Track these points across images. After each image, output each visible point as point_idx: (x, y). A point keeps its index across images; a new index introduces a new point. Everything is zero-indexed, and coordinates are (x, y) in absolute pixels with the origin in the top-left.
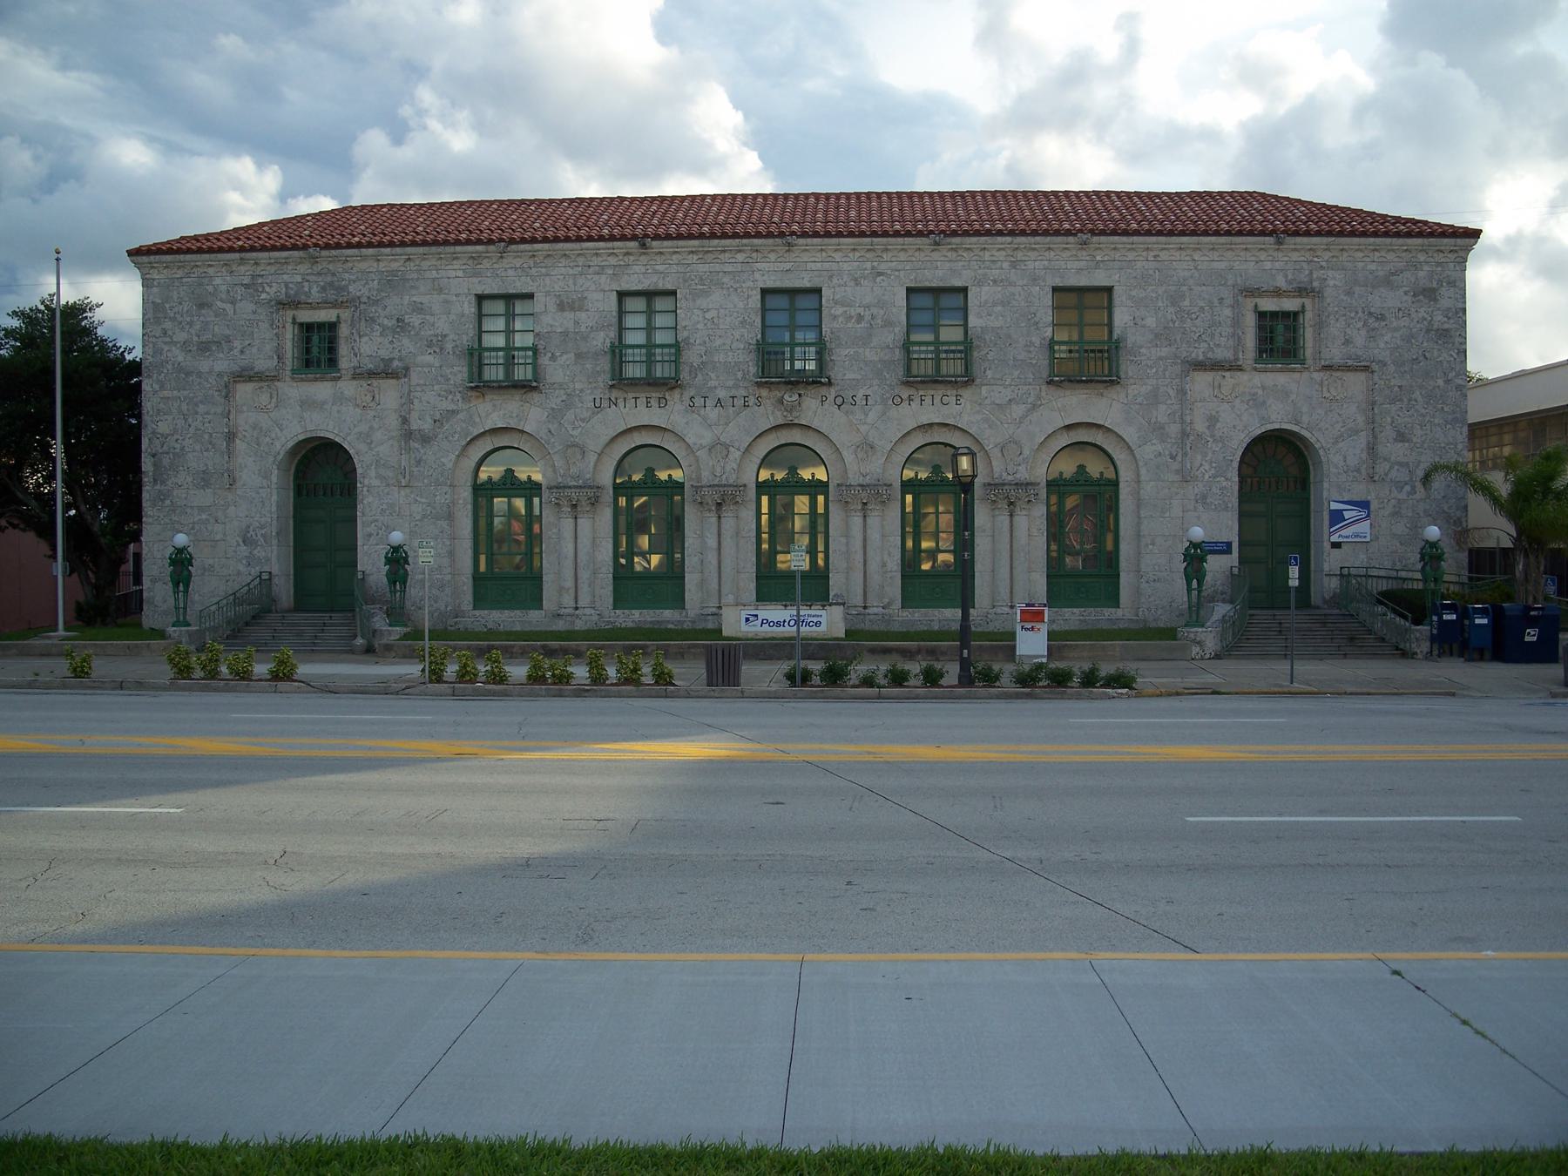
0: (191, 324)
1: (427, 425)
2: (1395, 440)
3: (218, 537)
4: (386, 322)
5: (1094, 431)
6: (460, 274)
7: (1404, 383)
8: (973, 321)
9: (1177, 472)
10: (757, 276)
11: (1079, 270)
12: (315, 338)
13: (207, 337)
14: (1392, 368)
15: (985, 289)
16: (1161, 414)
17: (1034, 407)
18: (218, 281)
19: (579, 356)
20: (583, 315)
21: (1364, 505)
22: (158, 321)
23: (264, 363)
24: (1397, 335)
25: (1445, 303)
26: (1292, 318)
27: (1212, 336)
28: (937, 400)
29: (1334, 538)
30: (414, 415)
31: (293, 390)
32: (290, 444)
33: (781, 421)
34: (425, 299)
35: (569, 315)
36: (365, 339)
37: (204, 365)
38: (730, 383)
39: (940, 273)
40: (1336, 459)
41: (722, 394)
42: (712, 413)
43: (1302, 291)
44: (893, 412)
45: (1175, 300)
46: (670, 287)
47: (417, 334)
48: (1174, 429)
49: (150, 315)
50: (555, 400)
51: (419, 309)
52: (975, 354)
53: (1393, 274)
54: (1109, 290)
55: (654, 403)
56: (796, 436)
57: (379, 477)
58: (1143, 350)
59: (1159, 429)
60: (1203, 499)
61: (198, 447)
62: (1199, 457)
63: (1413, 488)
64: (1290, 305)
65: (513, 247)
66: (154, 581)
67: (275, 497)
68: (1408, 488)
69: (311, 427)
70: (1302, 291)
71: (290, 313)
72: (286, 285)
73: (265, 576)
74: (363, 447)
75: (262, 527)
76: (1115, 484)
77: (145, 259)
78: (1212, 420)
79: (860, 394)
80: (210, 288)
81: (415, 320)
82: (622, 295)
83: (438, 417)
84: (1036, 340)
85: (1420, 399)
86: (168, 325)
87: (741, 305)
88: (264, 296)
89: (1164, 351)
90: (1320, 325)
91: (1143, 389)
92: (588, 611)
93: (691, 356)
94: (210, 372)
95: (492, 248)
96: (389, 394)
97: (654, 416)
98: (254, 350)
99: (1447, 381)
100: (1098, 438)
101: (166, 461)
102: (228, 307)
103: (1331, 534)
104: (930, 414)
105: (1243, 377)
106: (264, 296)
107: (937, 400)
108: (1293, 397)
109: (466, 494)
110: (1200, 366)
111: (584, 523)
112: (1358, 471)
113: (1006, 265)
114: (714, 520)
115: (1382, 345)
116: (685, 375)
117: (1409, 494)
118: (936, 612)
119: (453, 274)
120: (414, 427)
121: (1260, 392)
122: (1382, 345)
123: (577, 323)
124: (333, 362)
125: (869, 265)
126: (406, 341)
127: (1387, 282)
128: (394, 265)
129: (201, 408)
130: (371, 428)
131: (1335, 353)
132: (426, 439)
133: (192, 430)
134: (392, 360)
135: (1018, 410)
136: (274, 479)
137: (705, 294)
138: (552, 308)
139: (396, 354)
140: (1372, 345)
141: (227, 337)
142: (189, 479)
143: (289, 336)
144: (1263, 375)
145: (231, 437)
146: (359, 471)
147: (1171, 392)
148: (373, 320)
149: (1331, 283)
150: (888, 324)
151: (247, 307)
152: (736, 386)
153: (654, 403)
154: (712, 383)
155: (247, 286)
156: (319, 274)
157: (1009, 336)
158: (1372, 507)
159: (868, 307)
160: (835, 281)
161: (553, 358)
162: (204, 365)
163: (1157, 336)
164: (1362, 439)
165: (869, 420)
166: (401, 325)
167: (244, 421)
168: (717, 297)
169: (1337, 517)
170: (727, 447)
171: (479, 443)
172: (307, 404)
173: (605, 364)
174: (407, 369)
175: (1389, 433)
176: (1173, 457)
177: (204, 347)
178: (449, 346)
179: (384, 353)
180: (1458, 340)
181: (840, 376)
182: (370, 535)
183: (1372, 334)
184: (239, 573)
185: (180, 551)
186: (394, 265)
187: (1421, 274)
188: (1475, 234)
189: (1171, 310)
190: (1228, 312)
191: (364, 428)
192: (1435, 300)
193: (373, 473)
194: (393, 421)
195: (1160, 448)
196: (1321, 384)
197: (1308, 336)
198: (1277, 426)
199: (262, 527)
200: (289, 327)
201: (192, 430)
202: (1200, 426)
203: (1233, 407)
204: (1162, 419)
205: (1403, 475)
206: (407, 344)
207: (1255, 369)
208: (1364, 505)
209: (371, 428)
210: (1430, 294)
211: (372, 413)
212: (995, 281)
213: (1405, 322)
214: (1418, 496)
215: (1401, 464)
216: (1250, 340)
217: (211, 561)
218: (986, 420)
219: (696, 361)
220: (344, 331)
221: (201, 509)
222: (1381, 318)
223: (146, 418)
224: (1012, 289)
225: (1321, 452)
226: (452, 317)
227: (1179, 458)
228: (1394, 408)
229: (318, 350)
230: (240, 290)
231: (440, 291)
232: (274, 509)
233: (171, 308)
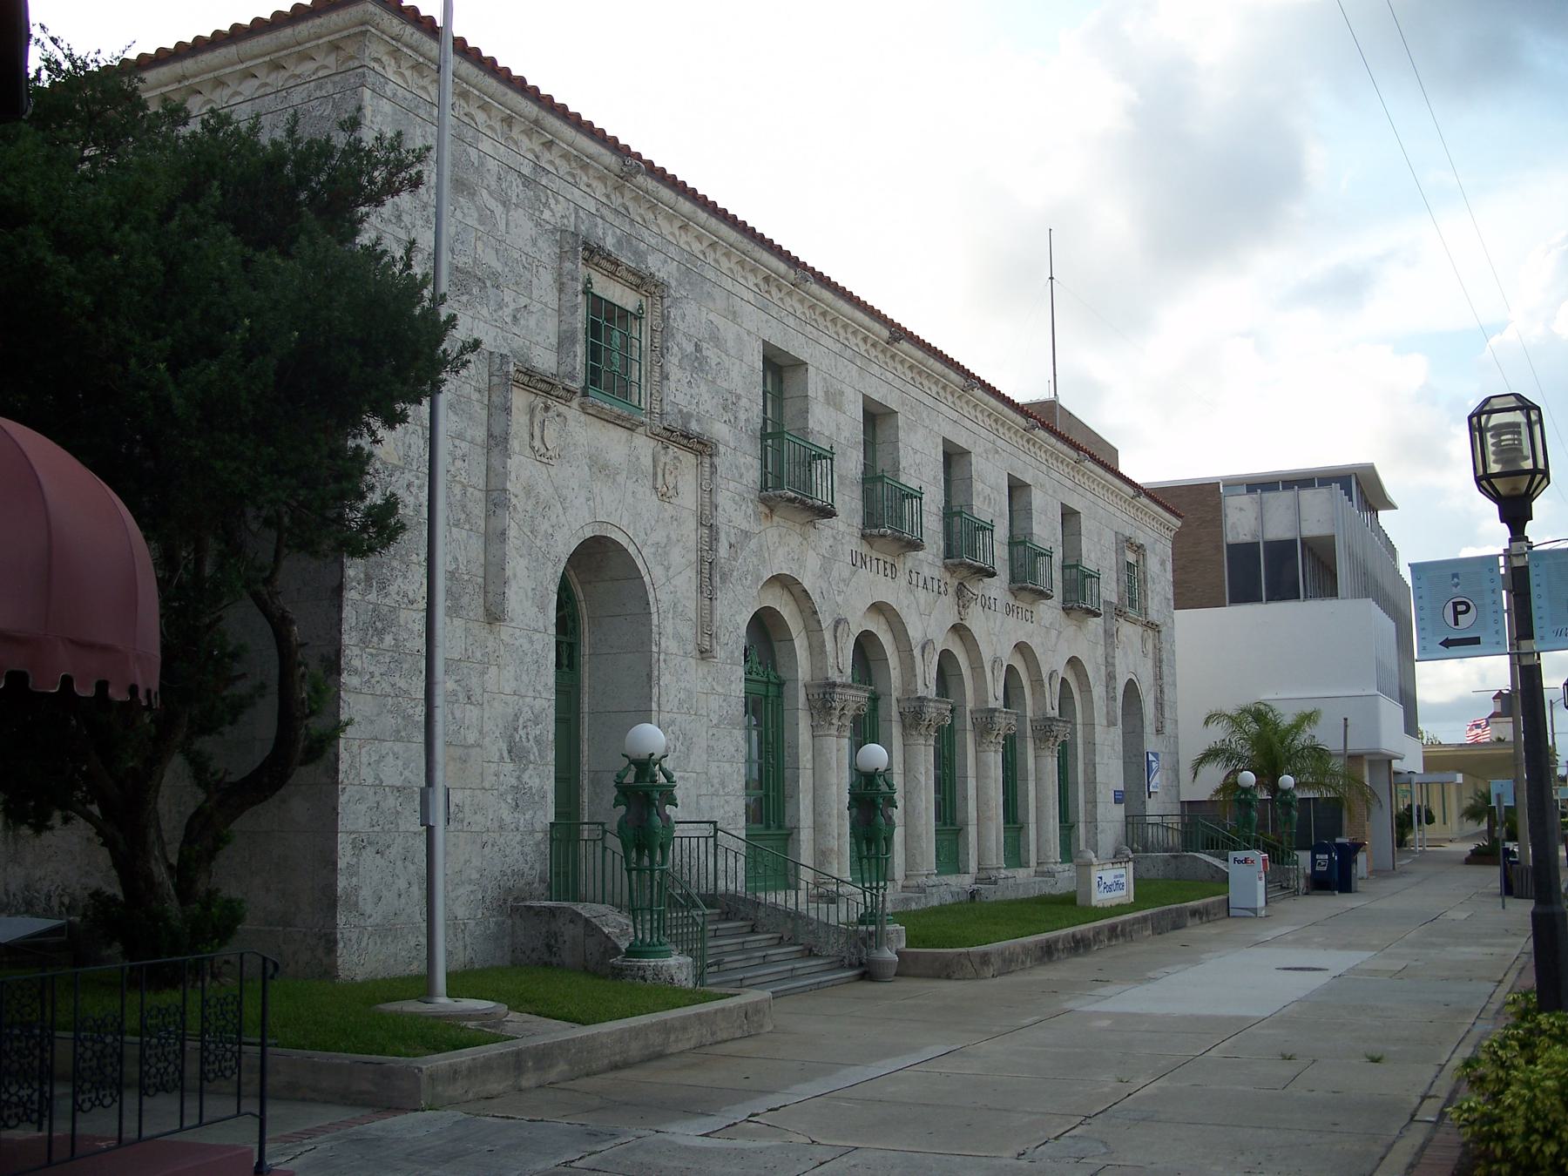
18: (486, 146)
66: (358, 847)
102: (499, 210)
126: (703, 388)
128: (697, 247)
134: (690, 415)
141: (495, 275)
186: (697, 247)
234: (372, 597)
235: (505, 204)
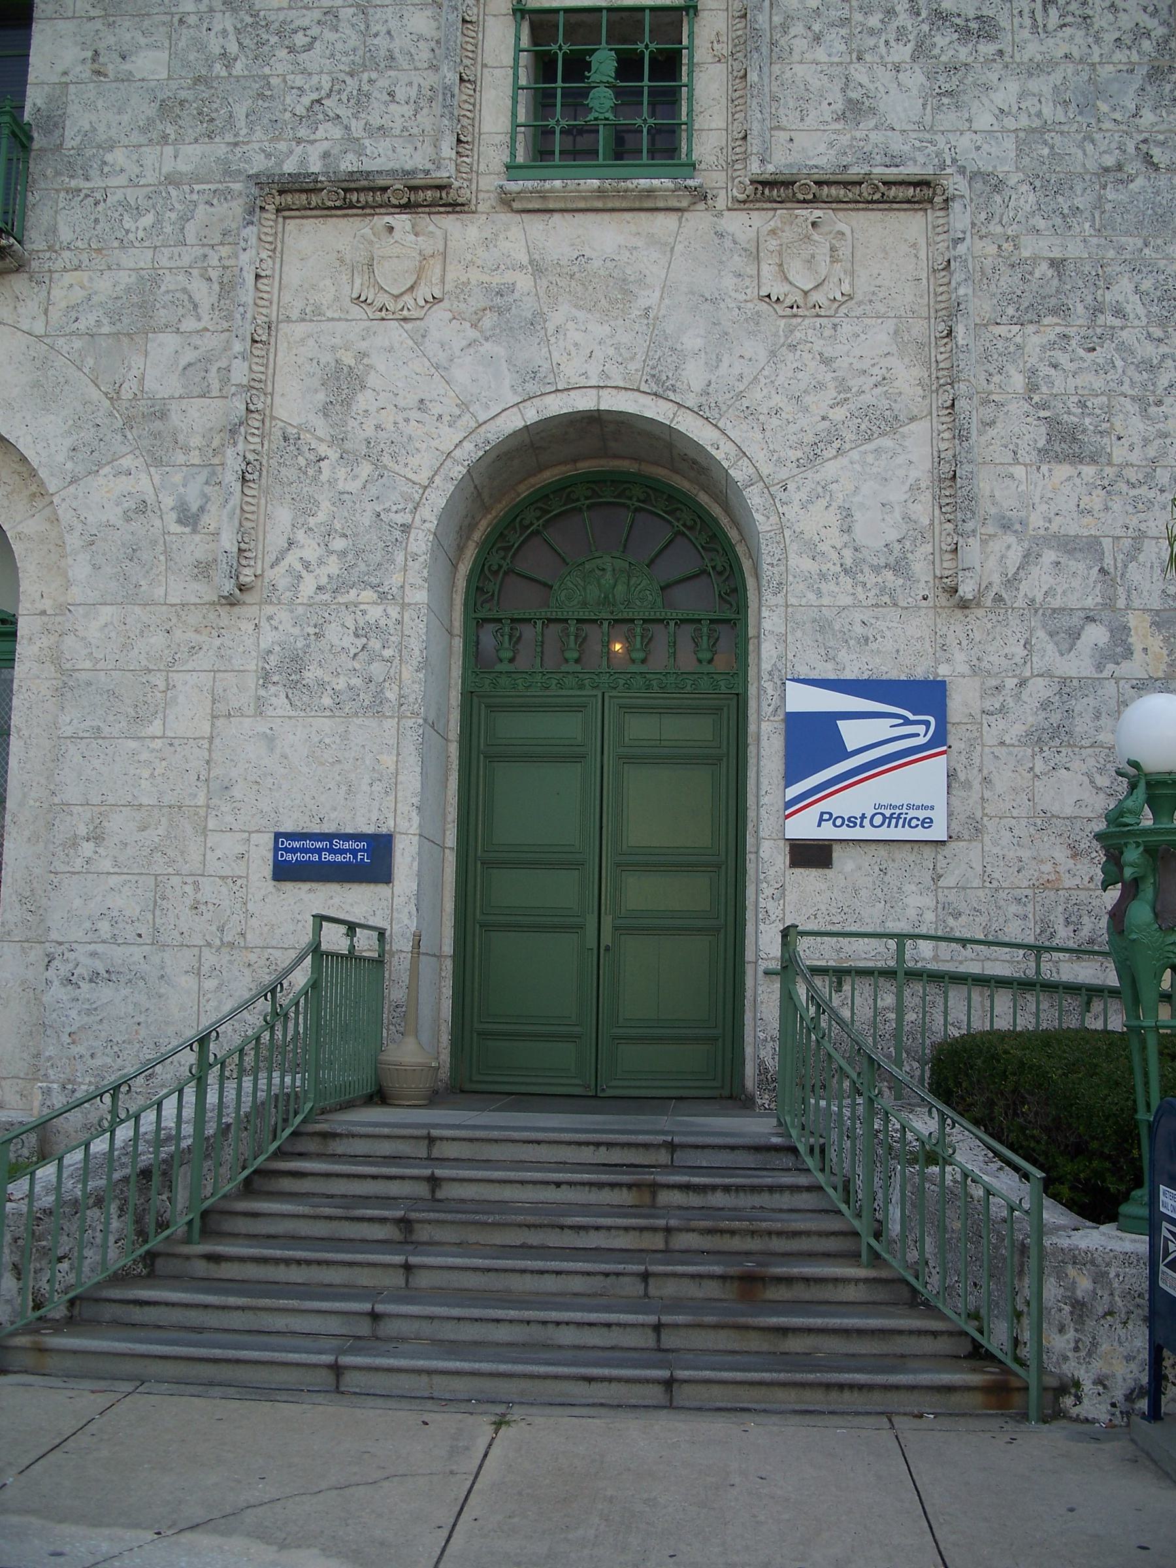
2: (1045, 454)
7: (1075, 250)
9: (203, 569)
14: (1026, 199)
21: (924, 697)
24: (1042, 85)
27: (361, 100)
29: (804, 827)
40: (816, 521)
48: (197, 418)
58: (118, 157)
59: (145, 421)
60: (289, 671)
63: (1119, 634)
68: (1096, 635)
78: (343, 384)
85: (1134, 306)
91: (104, 286)
108: (649, 298)
110: (296, 195)
112: (899, 567)
115: (984, 120)
121: (524, 282)
122: (984, 120)
131: (809, 147)
140: (949, 119)
144: (536, 226)
158: (962, 701)
163: (168, 108)
164: (917, 449)
169: (812, 742)
175: (1019, 427)
176: (189, 518)
183: (948, 90)
189: (225, 21)
195: (143, 484)
197: (708, 86)
198: (584, 402)
202: (294, 402)
204: (172, 385)
205: (1077, 588)
207: (507, 201)
214: (1134, 668)
215: (1069, 545)
216: (499, 105)
225: (754, 498)
228: (1034, 340)
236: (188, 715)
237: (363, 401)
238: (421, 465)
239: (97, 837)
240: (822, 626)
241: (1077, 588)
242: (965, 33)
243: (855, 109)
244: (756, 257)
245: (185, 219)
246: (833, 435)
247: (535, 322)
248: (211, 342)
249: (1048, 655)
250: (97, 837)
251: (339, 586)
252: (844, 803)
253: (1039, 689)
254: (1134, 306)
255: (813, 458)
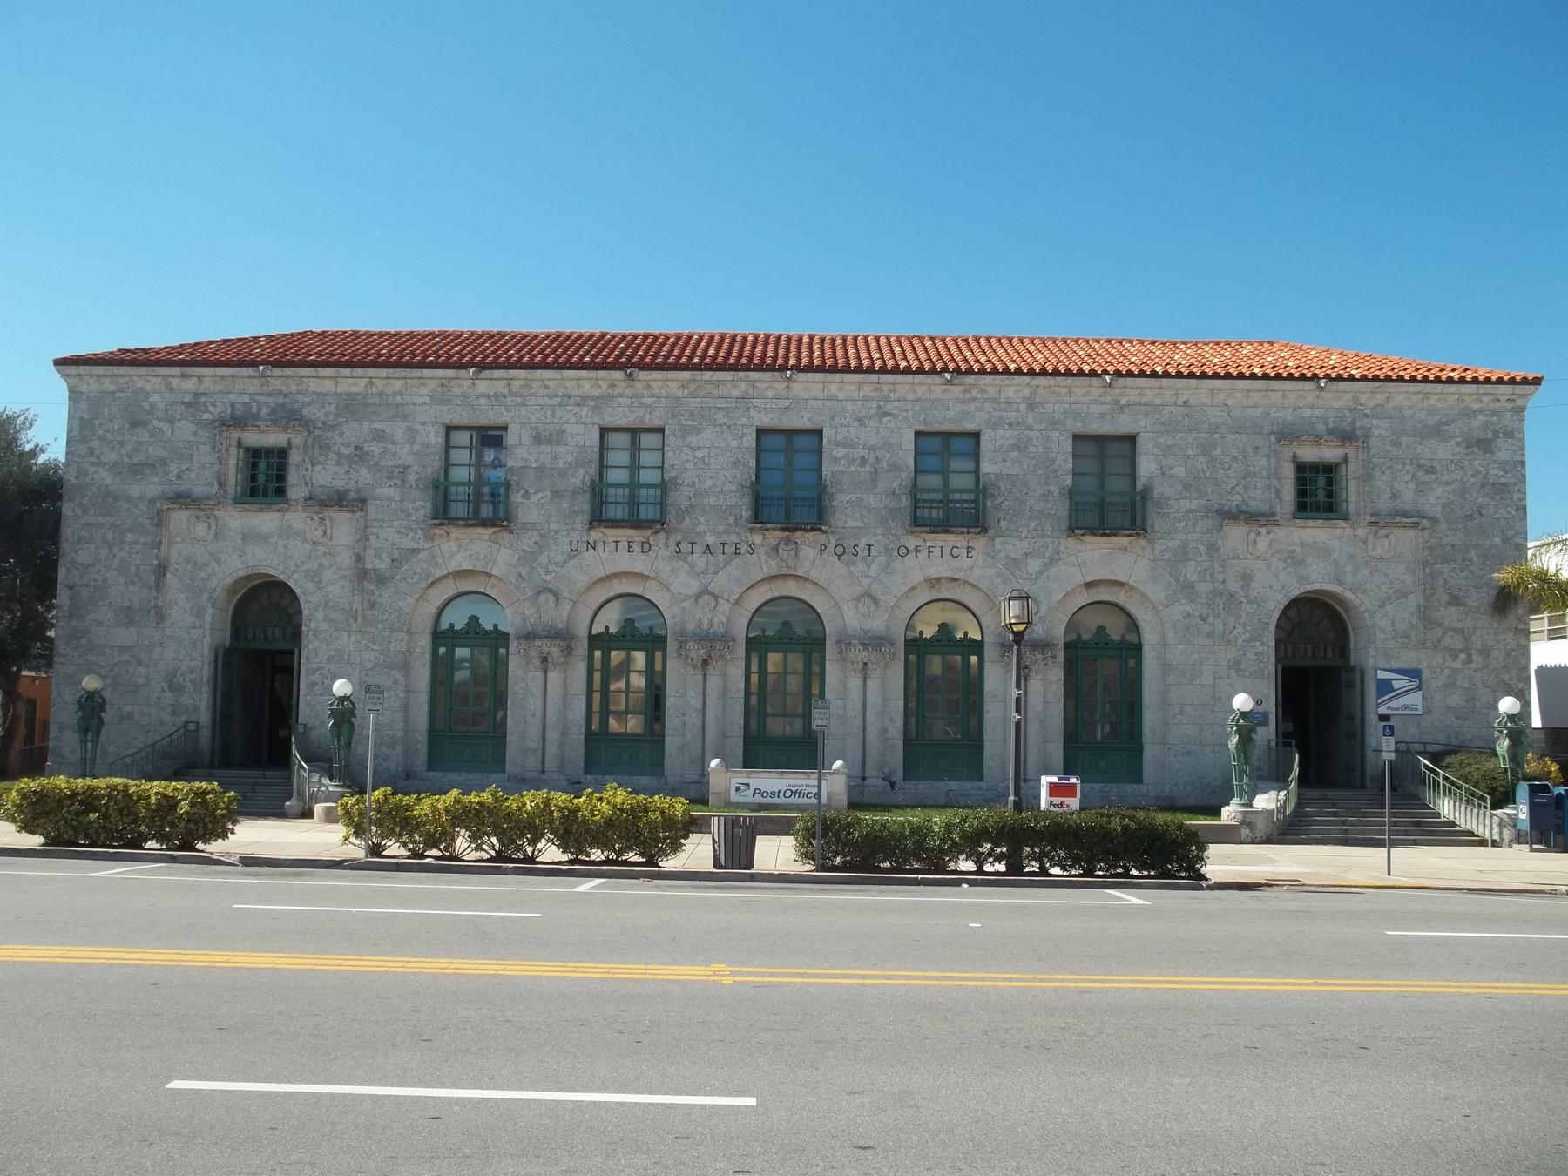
0: (122, 443)
1: (383, 565)
2: (1449, 604)
3: (141, 681)
4: (342, 449)
5: (1116, 588)
6: (427, 400)
7: (1458, 541)
8: (986, 467)
10: (752, 413)
11: (1102, 416)
12: (262, 465)
13: (135, 460)
14: (1444, 526)
15: (1000, 433)
16: (1190, 571)
17: (1052, 562)
18: (155, 398)
19: (556, 494)
20: (561, 449)
21: (1414, 674)
22: (84, 439)
23: (199, 490)
25: (1502, 455)
26: (1329, 470)
27: (1246, 488)
28: (946, 551)
29: (1383, 710)
30: (371, 552)
31: (237, 520)
32: (229, 581)
33: (774, 572)
34: (387, 427)
35: (546, 449)
36: (317, 468)
37: (135, 490)
38: (721, 528)
39: (951, 414)
40: (1385, 623)
41: (711, 539)
42: (700, 561)
43: (1345, 437)
44: (899, 564)
45: (1205, 450)
46: (657, 423)
47: (376, 464)
48: (1204, 588)
49: (75, 432)
50: (529, 541)
51: (380, 436)
52: (989, 503)
53: (1444, 424)
54: (1131, 439)
55: (636, 548)
56: (790, 588)
57: (327, 620)
59: (1188, 588)
60: (1236, 665)
61: (122, 580)
62: (1232, 619)
63: (1469, 656)
64: (1330, 453)
65: (487, 373)
66: (62, 729)
67: (207, 639)
68: (1463, 656)
69: (252, 562)
70: (1346, 437)
71: (235, 434)
72: (232, 405)
73: (192, 727)
74: (310, 586)
75: (192, 672)
76: (1137, 648)
77: (73, 370)
78: (1247, 579)
79: (863, 543)
80: (146, 406)
81: (375, 449)
82: (604, 431)
83: (396, 556)
84: (1055, 489)
85: (1475, 559)
86: (95, 444)
87: (734, 444)
88: (206, 416)
89: (1194, 504)
90: (1368, 477)
92: (555, 776)
93: (679, 498)
94: (141, 498)
95: (462, 373)
96: (343, 527)
97: (639, 563)
98: (193, 475)
99: (1506, 541)
100: (1121, 597)
101: (85, 594)
102: (166, 427)
103: (1378, 705)
104: (939, 568)
105: (1280, 532)
106: (206, 416)
107: (946, 551)
108: (1335, 555)
109: (425, 642)
111: (553, 677)
112: (1408, 636)
113: (1023, 407)
114: (700, 677)
116: (671, 518)
117: (1465, 663)
118: (941, 784)
119: (419, 400)
120: (369, 566)
121: (1299, 550)
122: (1432, 500)
123: (554, 458)
124: (281, 492)
125: (874, 404)
126: (364, 472)
127: (1438, 431)
129: (129, 537)
130: (321, 565)
132: (382, 580)
133: (117, 561)
134: (348, 491)
135: (1034, 565)
136: (208, 618)
137: (697, 430)
138: (526, 440)
139: (352, 485)
142: (110, 615)
143: (233, 461)
145: (161, 570)
146: (305, 613)
147: (1201, 547)
148: (328, 447)
149: (1377, 432)
150: (894, 468)
151: (185, 429)
152: (728, 532)
153: (636, 548)
154: (700, 528)
155: (188, 405)
156: (270, 394)
157: (1026, 484)
158: (1426, 675)
159: (872, 449)
160: (837, 420)
161: (527, 495)
162: (135, 490)
163: (1186, 487)
164: (1413, 602)
165: (872, 573)
166: (359, 454)
167: (176, 553)
168: (708, 435)
169: (1385, 687)
170: (716, 597)
171: (440, 586)
172: (248, 536)
173: (584, 504)
174: (363, 501)
175: (1442, 596)
176: (1204, 619)
177: (137, 470)
178: (412, 478)
179: (340, 484)
180: (1516, 496)
181: (840, 524)
182: (314, 684)
184: (162, 723)
185: (91, 695)
187: (1475, 424)
188: (1537, 381)
189: (1202, 459)
190: (1264, 462)
191: (312, 565)
192: (1492, 452)
193: (320, 615)
194: (345, 560)
195: (1189, 608)
196: (1365, 542)
198: (1317, 587)
199: (192, 672)
200: (234, 451)
201: (117, 561)
203: (1269, 566)
204: (1194, 578)
205: (1458, 643)
206: (365, 476)
208: (1414, 674)
209: (321, 565)
210: (1484, 445)
211: (321, 549)
212: (1011, 425)
213: (1458, 475)
214: (1473, 666)
215: (1455, 630)
217: (130, 709)
218: (999, 575)
219: (684, 504)
220: (294, 458)
221: (122, 649)
222: (1432, 470)
223: (65, 546)
224: (1030, 434)
225: (1367, 616)
226: (417, 447)
227: (1210, 620)
228: (1446, 569)
229: (265, 478)
230: (180, 409)
231: (405, 418)
232: (206, 652)
233: (101, 425)
234: (74, 623)
235: (171, 421)
236: (1207, 678)
237: (1254, 585)
238: (1271, 605)
239: (1182, 713)
240: (1386, 654)
241: (1458, 643)
242: (1426, 472)
243: (1394, 496)
244: (1365, 542)
245: (1195, 524)
246: (1389, 598)
247: (1303, 562)
248: (1207, 564)
249: (1449, 661)
250: (1182, 713)
251: (1249, 641)
252: (1394, 704)
253: (1447, 672)
254: (1475, 559)
255: (1382, 606)
